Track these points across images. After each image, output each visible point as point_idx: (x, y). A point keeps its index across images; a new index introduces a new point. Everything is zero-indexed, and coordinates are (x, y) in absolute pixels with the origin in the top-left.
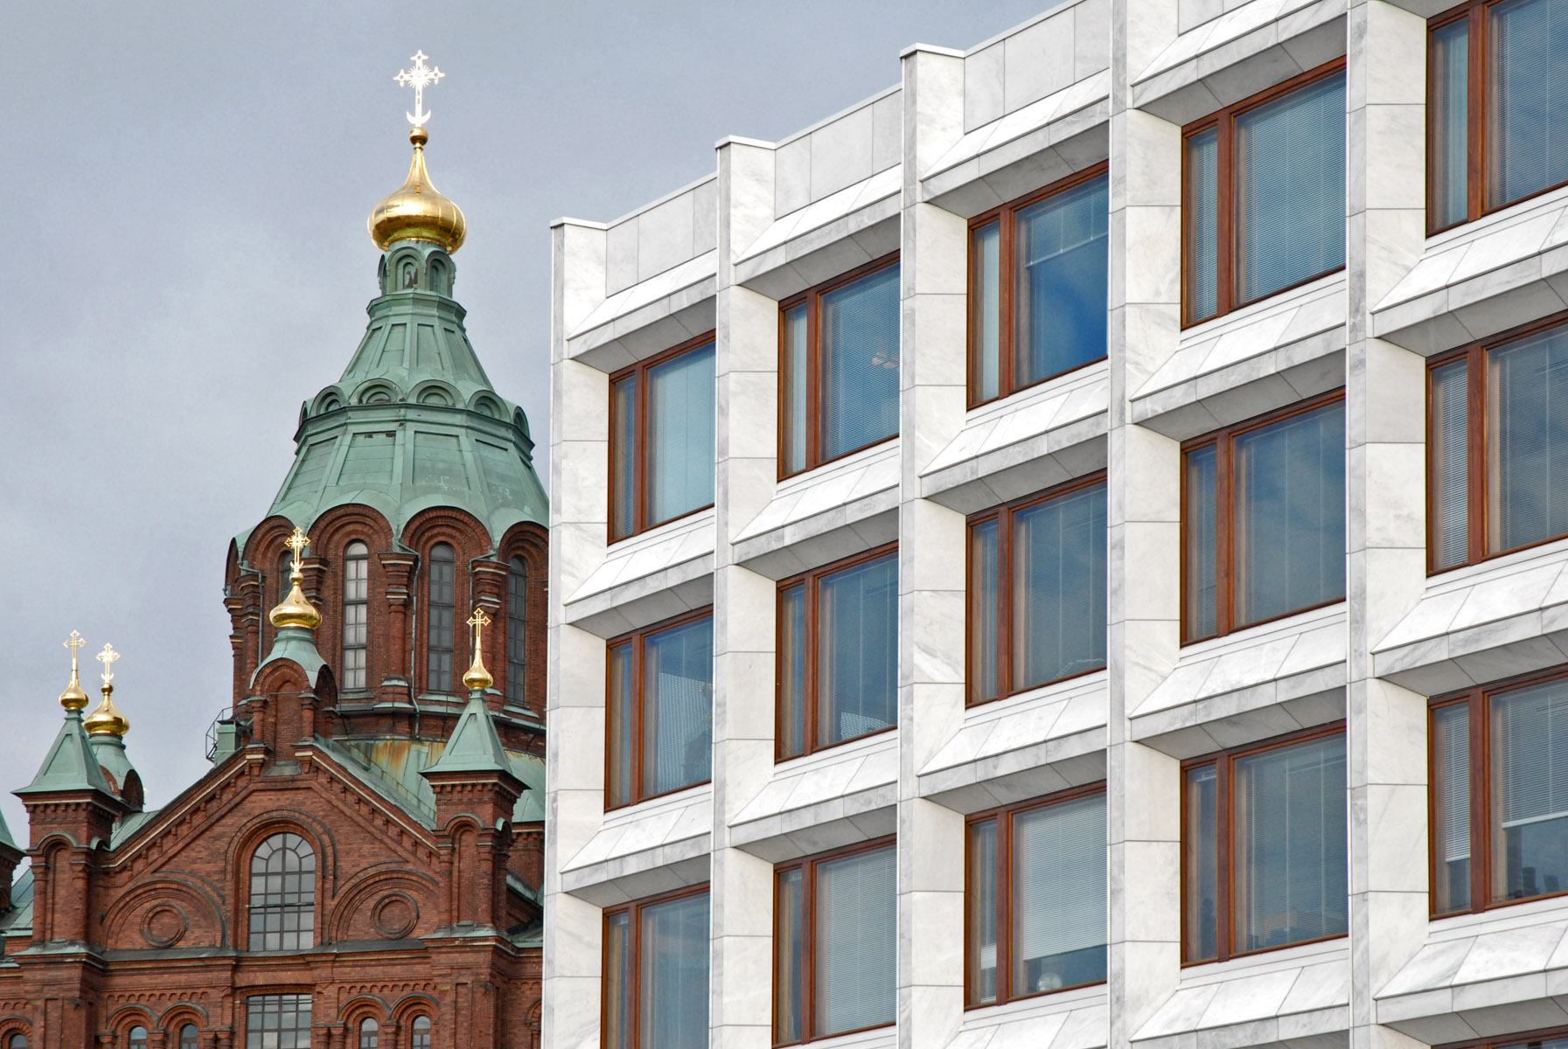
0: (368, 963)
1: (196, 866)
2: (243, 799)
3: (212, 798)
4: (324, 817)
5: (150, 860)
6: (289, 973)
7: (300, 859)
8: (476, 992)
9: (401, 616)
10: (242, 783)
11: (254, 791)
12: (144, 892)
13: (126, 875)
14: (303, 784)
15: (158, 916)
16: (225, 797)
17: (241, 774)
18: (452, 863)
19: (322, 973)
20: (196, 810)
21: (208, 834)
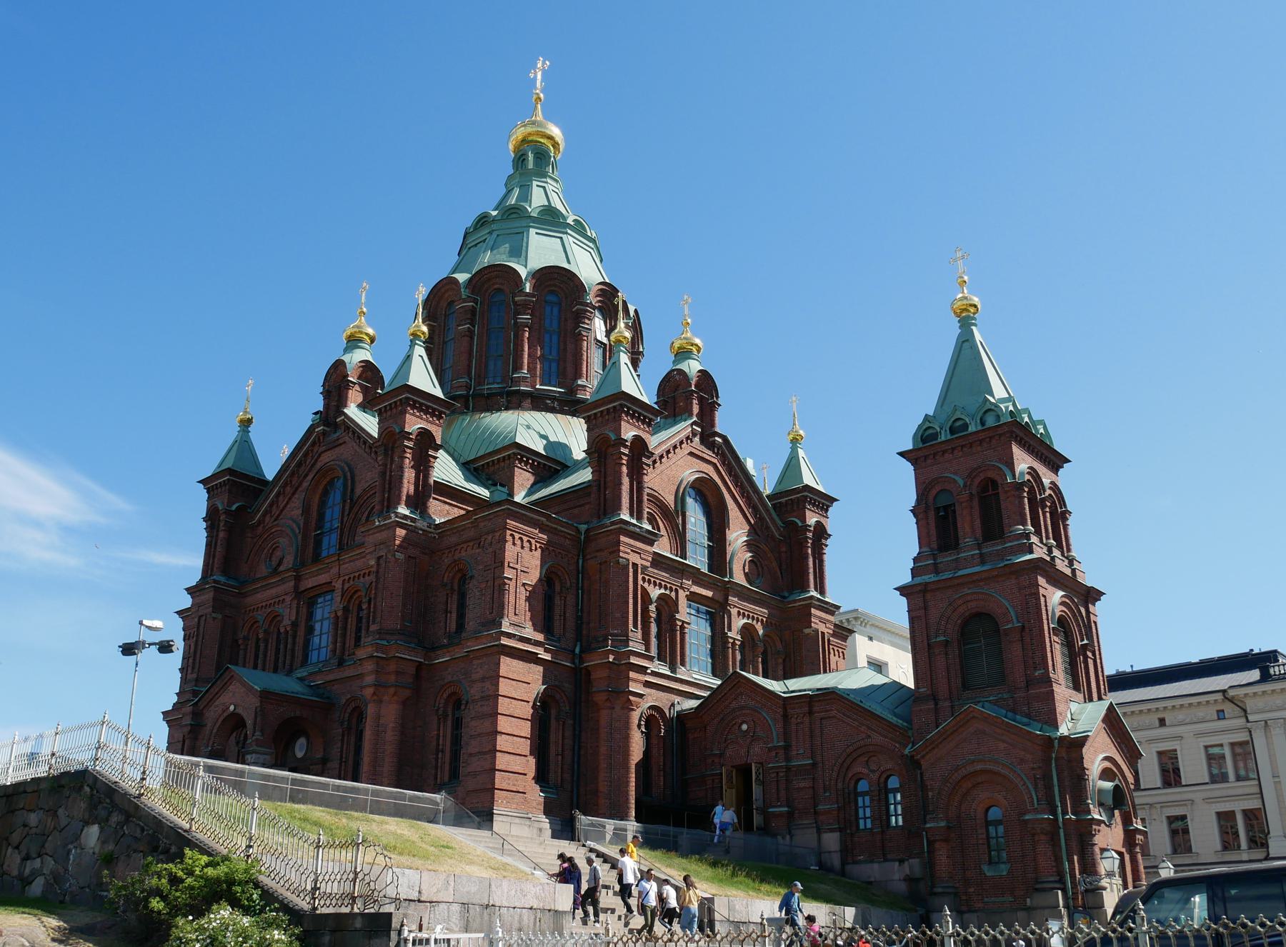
0: (355, 557)
1: (293, 513)
2: (316, 460)
3: (299, 465)
4: (351, 460)
5: (273, 513)
6: (323, 576)
8: (389, 562)
9: (467, 339)
10: (316, 449)
12: (268, 536)
13: (260, 528)
14: (341, 441)
15: (275, 552)
16: (308, 462)
17: (314, 444)
18: (386, 465)
19: (335, 570)
20: (292, 474)
21: (300, 489)
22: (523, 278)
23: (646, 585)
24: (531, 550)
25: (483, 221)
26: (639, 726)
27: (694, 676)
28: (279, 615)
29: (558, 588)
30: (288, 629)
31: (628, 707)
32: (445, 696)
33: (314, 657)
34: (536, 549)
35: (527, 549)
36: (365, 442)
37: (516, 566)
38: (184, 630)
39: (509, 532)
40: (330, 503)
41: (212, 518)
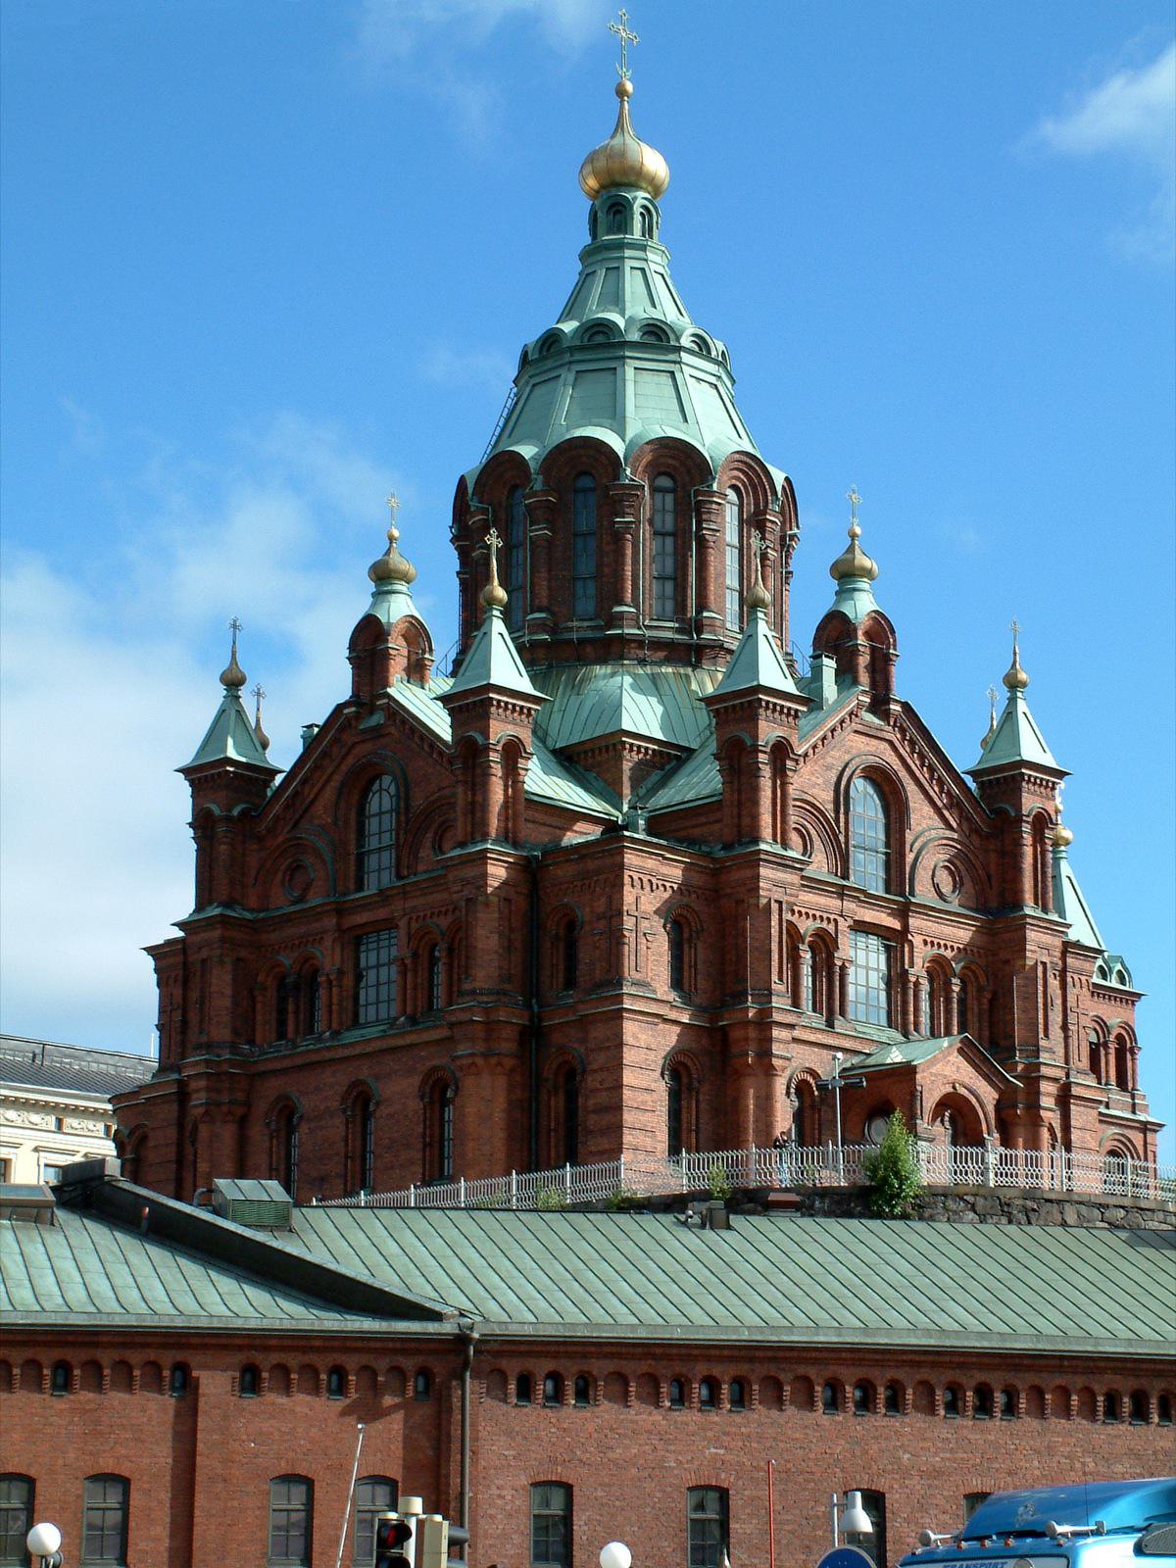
7: (391, 797)
11: (355, 744)
22: (621, 456)
23: (795, 919)
24: (652, 891)
25: (551, 341)
26: (788, 1094)
27: (859, 1028)
28: (312, 958)
29: (686, 935)
30: (332, 977)
31: (769, 1072)
32: (554, 1066)
33: (368, 1014)
34: (658, 888)
35: (648, 888)
36: (441, 753)
37: (636, 914)
38: (156, 970)
39: (627, 873)
40: (373, 806)
41: (202, 824)
